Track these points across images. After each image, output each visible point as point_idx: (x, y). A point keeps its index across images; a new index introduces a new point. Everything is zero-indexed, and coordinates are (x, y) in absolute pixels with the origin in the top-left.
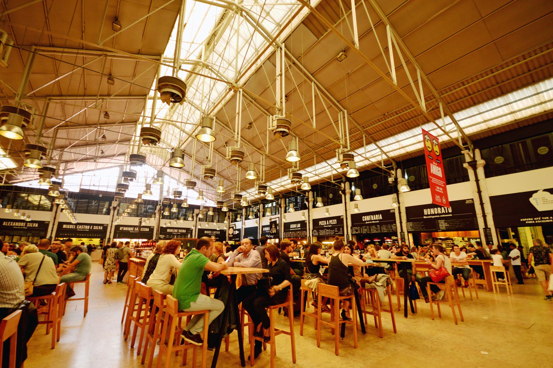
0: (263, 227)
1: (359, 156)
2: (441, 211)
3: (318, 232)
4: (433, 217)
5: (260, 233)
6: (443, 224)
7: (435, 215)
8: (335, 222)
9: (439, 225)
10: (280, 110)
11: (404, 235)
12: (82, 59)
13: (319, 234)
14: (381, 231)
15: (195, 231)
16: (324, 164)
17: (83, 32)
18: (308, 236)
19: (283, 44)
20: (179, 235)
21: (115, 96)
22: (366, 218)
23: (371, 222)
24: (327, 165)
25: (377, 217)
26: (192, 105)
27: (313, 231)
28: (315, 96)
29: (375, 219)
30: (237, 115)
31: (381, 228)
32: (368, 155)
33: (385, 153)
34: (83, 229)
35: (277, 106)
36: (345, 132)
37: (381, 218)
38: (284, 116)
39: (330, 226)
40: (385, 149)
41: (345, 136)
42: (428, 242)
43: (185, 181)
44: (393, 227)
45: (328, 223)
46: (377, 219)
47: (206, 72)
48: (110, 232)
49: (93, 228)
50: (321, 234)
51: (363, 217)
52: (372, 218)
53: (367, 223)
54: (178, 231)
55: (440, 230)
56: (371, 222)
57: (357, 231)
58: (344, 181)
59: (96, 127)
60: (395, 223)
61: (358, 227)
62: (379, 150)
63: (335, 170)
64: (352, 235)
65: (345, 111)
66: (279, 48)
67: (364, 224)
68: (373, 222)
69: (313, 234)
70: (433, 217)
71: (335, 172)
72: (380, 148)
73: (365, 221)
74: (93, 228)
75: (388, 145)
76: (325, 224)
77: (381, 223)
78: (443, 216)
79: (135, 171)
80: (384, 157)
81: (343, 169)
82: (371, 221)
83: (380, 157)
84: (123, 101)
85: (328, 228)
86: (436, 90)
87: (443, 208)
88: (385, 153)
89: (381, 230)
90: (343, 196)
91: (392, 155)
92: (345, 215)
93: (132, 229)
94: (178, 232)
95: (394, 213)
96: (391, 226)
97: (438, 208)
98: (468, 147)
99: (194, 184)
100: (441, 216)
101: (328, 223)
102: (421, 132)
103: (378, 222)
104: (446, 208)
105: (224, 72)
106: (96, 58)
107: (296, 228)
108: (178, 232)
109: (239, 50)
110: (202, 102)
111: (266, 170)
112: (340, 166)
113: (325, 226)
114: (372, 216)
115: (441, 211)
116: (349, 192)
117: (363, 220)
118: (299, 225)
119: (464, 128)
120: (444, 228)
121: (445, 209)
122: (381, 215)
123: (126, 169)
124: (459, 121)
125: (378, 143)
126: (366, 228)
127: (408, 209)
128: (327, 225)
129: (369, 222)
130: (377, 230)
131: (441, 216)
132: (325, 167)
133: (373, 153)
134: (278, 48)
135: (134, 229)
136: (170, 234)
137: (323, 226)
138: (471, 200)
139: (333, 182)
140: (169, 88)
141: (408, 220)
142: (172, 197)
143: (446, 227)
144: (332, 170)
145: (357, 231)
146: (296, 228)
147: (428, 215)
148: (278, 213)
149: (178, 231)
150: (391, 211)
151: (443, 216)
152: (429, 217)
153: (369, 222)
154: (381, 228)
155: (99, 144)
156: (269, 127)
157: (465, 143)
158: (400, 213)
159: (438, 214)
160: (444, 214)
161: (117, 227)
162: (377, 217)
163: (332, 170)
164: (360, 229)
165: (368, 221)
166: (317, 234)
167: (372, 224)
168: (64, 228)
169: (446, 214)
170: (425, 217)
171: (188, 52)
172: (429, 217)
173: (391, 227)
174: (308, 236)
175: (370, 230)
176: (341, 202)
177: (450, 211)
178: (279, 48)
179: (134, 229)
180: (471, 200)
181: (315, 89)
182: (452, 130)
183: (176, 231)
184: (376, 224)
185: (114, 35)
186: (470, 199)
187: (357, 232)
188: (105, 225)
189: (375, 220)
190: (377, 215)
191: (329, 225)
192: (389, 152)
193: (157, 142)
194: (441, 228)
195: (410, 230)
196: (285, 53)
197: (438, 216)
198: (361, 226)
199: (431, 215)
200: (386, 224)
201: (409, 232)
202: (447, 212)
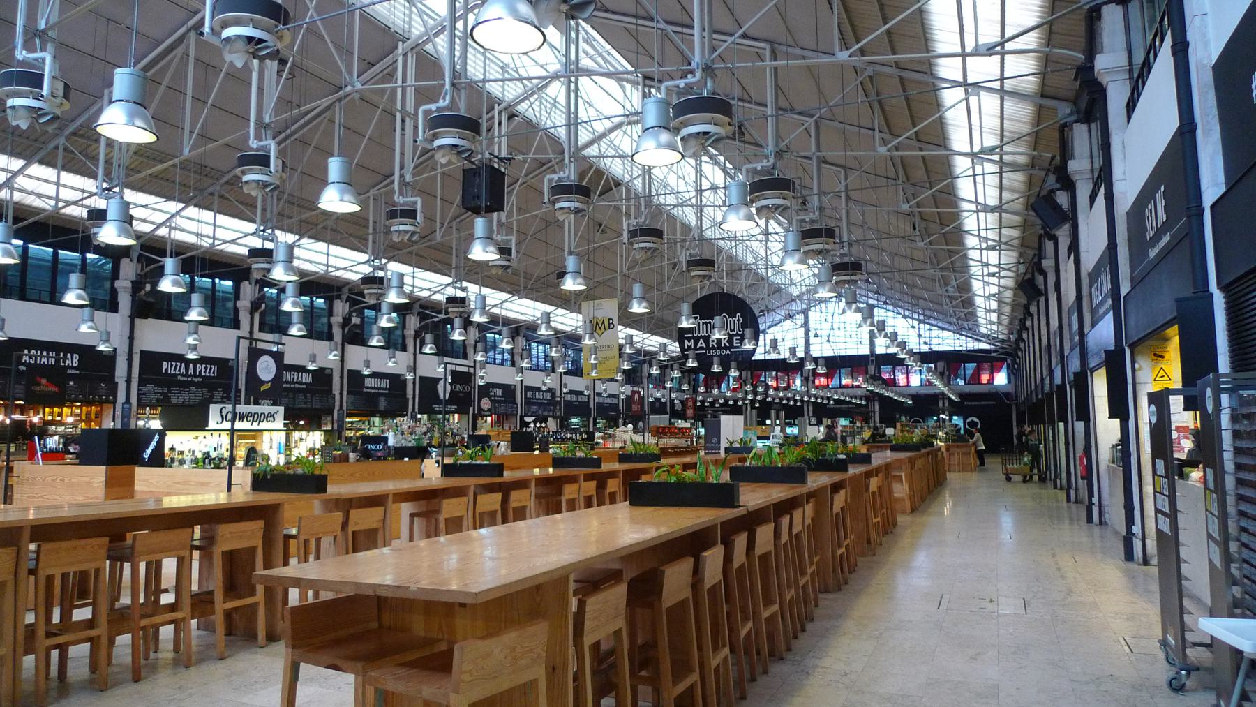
8: (212, 371)
23: (292, 386)
25: (304, 378)
37: (310, 380)
39: (196, 380)
45: (191, 371)
46: (304, 381)
52: (296, 377)
56: (292, 386)
68: (297, 386)
76: (183, 371)
77: (309, 390)
82: (294, 383)
95: (331, 376)
101: (191, 371)
103: (304, 386)
113: (179, 377)
128: (187, 375)
129: (289, 386)
137: (176, 375)
153: (289, 386)
162: (304, 378)
191: (195, 376)
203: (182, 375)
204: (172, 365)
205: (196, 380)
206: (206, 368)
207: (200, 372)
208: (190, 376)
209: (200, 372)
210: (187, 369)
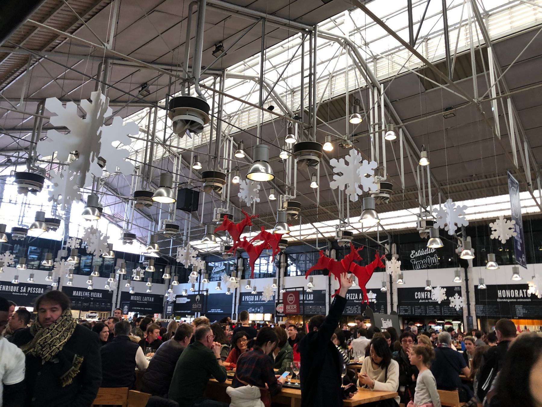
0: (242, 294)
2: (519, 294)
4: (509, 301)
5: (237, 305)
6: (520, 310)
7: (511, 298)
14: (441, 313)
15: (117, 296)
23: (427, 301)
31: (441, 309)
53: (421, 301)
55: (516, 317)
56: (427, 301)
57: (406, 311)
67: (417, 303)
70: (509, 301)
73: (418, 299)
76: (356, 297)
89: (441, 311)
97: (516, 291)
100: (518, 300)
113: (355, 301)
115: (519, 294)
117: (416, 298)
120: (521, 315)
121: (523, 293)
126: (419, 308)
128: (358, 299)
129: (424, 301)
130: (435, 312)
131: (518, 300)
135: (20, 289)
141: (477, 303)
143: (524, 313)
145: (406, 311)
147: (502, 298)
152: (504, 300)
153: (424, 301)
154: (441, 309)
159: (515, 298)
160: (521, 298)
165: (422, 299)
169: (524, 298)
170: (499, 300)
172: (504, 300)
175: (426, 311)
179: (20, 289)
187: (406, 312)
194: (518, 315)
195: (480, 314)
197: (515, 300)
199: (506, 298)
201: (477, 317)
202: (525, 296)
203: (356, 300)
204: (351, 295)
210: (358, 296)
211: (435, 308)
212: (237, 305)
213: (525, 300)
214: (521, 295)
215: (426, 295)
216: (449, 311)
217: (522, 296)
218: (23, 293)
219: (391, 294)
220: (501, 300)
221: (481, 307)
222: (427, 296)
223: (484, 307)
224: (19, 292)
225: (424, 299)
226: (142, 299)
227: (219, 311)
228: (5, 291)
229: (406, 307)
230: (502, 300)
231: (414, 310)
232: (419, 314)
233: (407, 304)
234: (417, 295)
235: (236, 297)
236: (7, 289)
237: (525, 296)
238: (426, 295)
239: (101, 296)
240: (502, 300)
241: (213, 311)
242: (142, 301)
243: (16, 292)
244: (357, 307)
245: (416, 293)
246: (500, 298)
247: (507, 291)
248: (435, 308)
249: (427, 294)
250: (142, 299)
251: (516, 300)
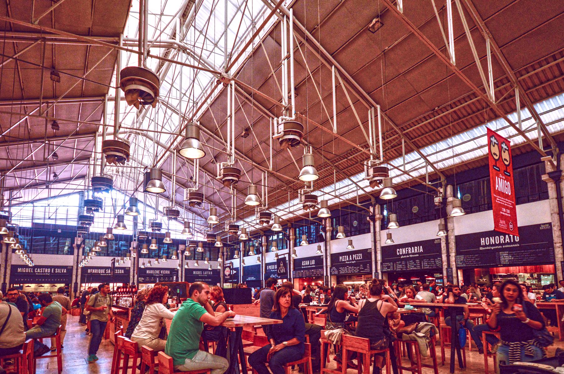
0: (267, 265)
1: (396, 170)
2: (505, 240)
3: (338, 269)
4: (493, 248)
5: (264, 273)
7: (495, 245)
8: (360, 256)
9: (500, 258)
10: (288, 109)
11: (452, 271)
12: (12, 45)
13: (339, 272)
15: (182, 272)
16: (347, 182)
17: (7, 5)
18: (325, 274)
19: (291, 10)
20: (161, 276)
21: (64, 98)
22: (402, 251)
23: (408, 256)
24: (350, 182)
25: (416, 250)
26: (167, 107)
27: (331, 268)
28: (336, 87)
29: (413, 251)
30: (229, 118)
32: (408, 167)
33: (432, 165)
34: (42, 273)
35: (283, 103)
36: (377, 136)
37: (421, 250)
38: (294, 117)
39: (353, 262)
40: (432, 159)
41: (378, 142)
42: (484, 280)
43: (165, 209)
44: (438, 262)
45: (351, 259)
47: (182, 57)
48: (77, 276)
49: (54, 271)
50: (341, 272)
51: (398, 250)
52: (410, 251)
53: (402, 257)
54: (160, 272)
56: (408, 256)
57: (389, 267)
58: (373, 203)
59: (43, 142)
60: (441, 257)
61: (390, 262)
62: (422, 160)
63: (362, 189)
64: (382, 272)
65: (378, 107)
66: (285, 17)
67: (399, 259)
68: (411, 256)
69: (331, 273)
70: (493, 248)
71: (361, 192)
72: (424, 157)
73: (400, 255)
74: (54, 271)
75: (437, 152)
76: (347, 259)
77: (421, 257)
78: (508, 246)
79: (101, 199)
80: (430, 169)
81: (373, 187)
82: (408, 254)
83: (424, 169)
84: (75, 103)
85: (350, 265)
86: (513, 70)
87: (507, 236)
88: (432, 165)
90: (372, 223)
91: (440, 166)
92: (373, 248)
93: (103, 271)
94: (160, 273)
96: (434, 260)
98: (551, 151)
99: (177, 213)
100: (504, 247)
101: (351, 259)
102: (485, 131)
104: (512, 236)
105: (208, 57)
106: (32, 44)
107: (310, 265)
108: (160, 273)
109: (228, 23)
110: (180, 102)
111: (269, 193)
112: (369, 184)
113: (346, 262)
114: (409, 248)
115: (505, 240)
116: (379, 218)
118: (313, 262)
119: (549, 124)
122: (421, 247)
123: (88, 195)
124: (542, 114)
125: (422, 151)
126: (400, 264)
127: (457, 237)
128: (349, 261)
129: (405, 257)
131: (504, 247)
132: (348, 186)
133: (415, 164)
134: (283, 16)
136: (151, 276)
137: (345, 262)
138: (548, 225)
139: (358, 205)
140: (135, 84)
141: (458, 253)
142: (149, 230)
144: (357, 190)
145: (389, 267)
146: (310, 265)
147: (486, 246)
148: (285, 246)
149: (160, 272)
150: (436, 242)
151: (508, 246)
152: (488, 248)
153: (405, 257)
155: (50, 164)
156: (273, 134)
157: (547, 145)
158: (447, 243)
159: (500, 244)
160: (508, 243)
161: (85, 269)
162: (416, 250)
163: (357, 190)
164: (393, 266)
165: (403, 255)
166: (336, 273)
167: (410, 259)
168: (19, 273)
169: (510, 243)
170: (481, 248)
171: (156, 29)
172: (488, 248)
173: (435, 262)
174: (325, 274)
176: (369, 232)
177: (517, 239)
178: (285, 17)
179: (105, 271)
180: (548, 225)
181: (336, 77)
182: (530, 128)
183: (157, 272)
184: (414, 259)
185: (52, 9)
186: (547, 224)
187: (388, 268)
188: (69, 268)
189: (413, 254)
190: (415, 247)
191: (353, 260)
192: (437, 162)
193: (125, 159)
196: (294, 23)
198: (394, 261)
199: (490, 245)
200: (429, 258)
202: (512, 241)
204: (357, 256)
205: (353, 262)
206: (357, 256)
207: (355, 258)
208: (351, 261)
209: (355, 258)
210: (349, 259)
211: (415, 263)
212: (264, 273)
213: (512, 246)
214: (507, 240)
215: (407, 251)
216: (428, 264)
217: (509, 242)
218: (108, 273)
219: (376, 252)
220: (484, 249)
221: (462, 257)
222: (408, 252)
223: (464, 257)
224: (105, 273)
225: (406, 255)
226: (202, 273)
227: (253, 278)
228: (95, 273)
229: (388, 264)
230: (486, 248)
231: (396, 265)
232: (400, 270)
233: (389, 261)
234: (399, 252)
235: (262, 267)
236: (96, 271)
237: (512, 241)
238: (407, 251)
239: (169, 273)
240: (486, 248)
241: (249, 279)
242: (203, 275)
243: (103, 273)
244: (347, 268)
245: (398, 250)
246: (483, 246)
247: (491, 238)
248: (415, 263)
249: (408, 249)
250: (202, 273)
251: (501, 247)
